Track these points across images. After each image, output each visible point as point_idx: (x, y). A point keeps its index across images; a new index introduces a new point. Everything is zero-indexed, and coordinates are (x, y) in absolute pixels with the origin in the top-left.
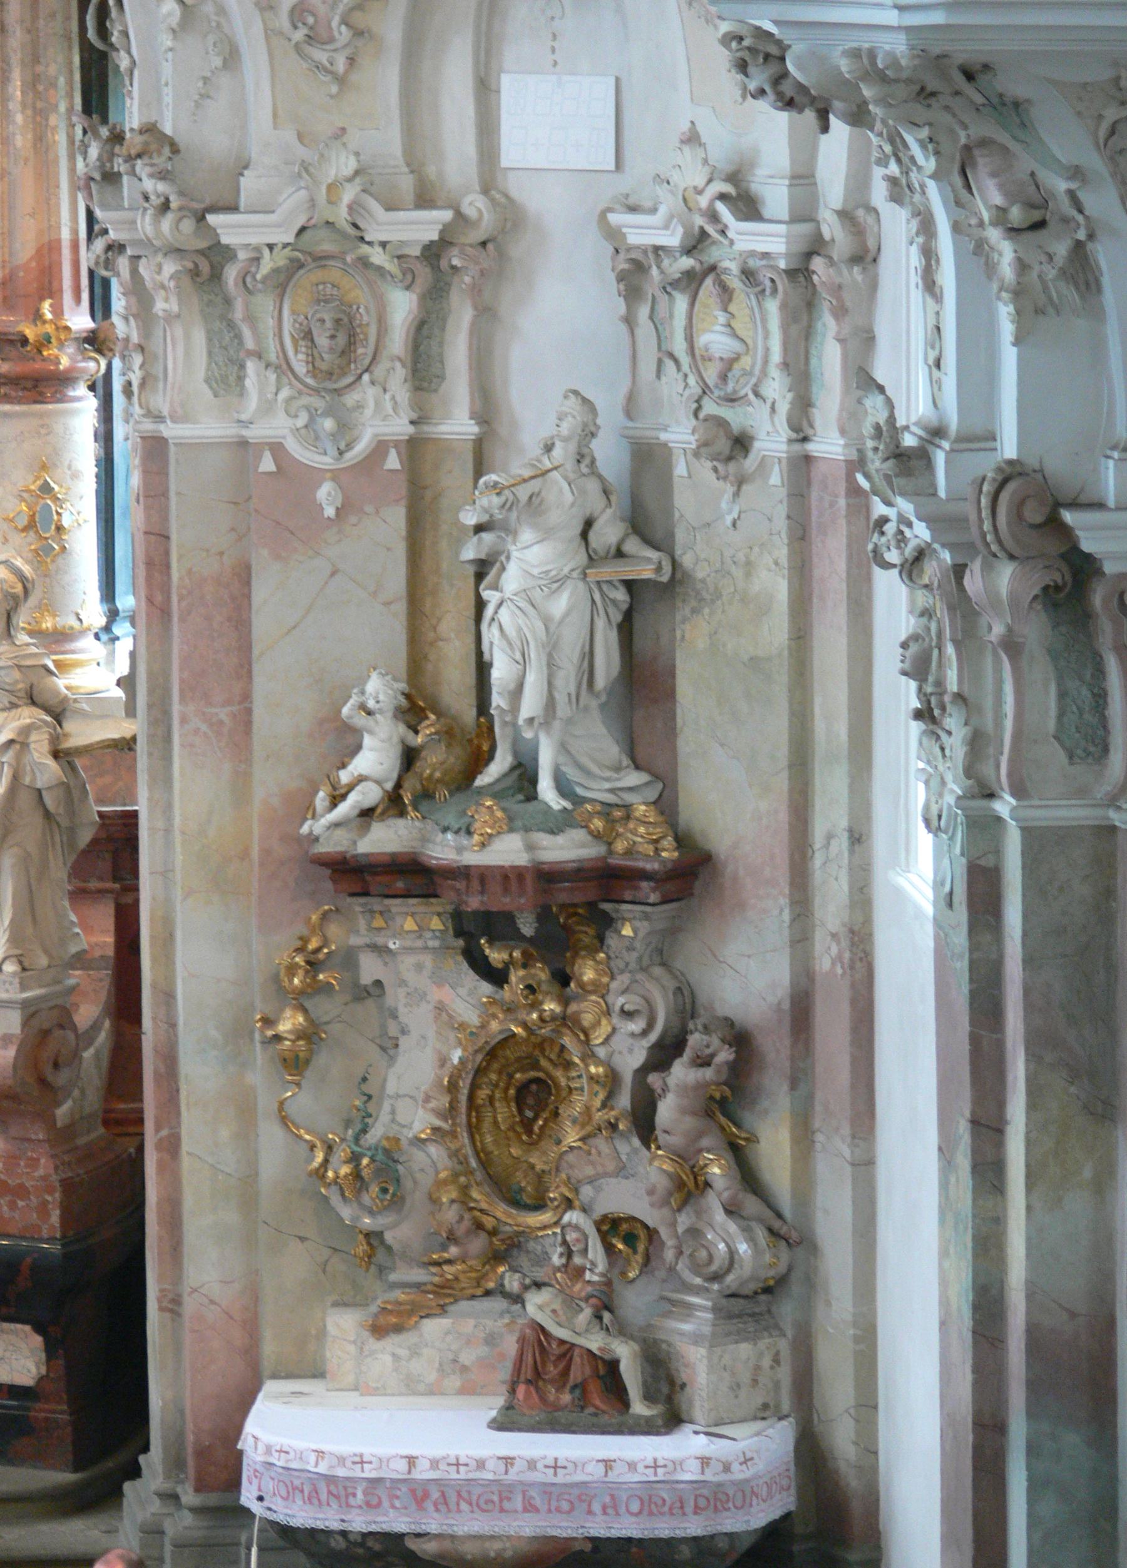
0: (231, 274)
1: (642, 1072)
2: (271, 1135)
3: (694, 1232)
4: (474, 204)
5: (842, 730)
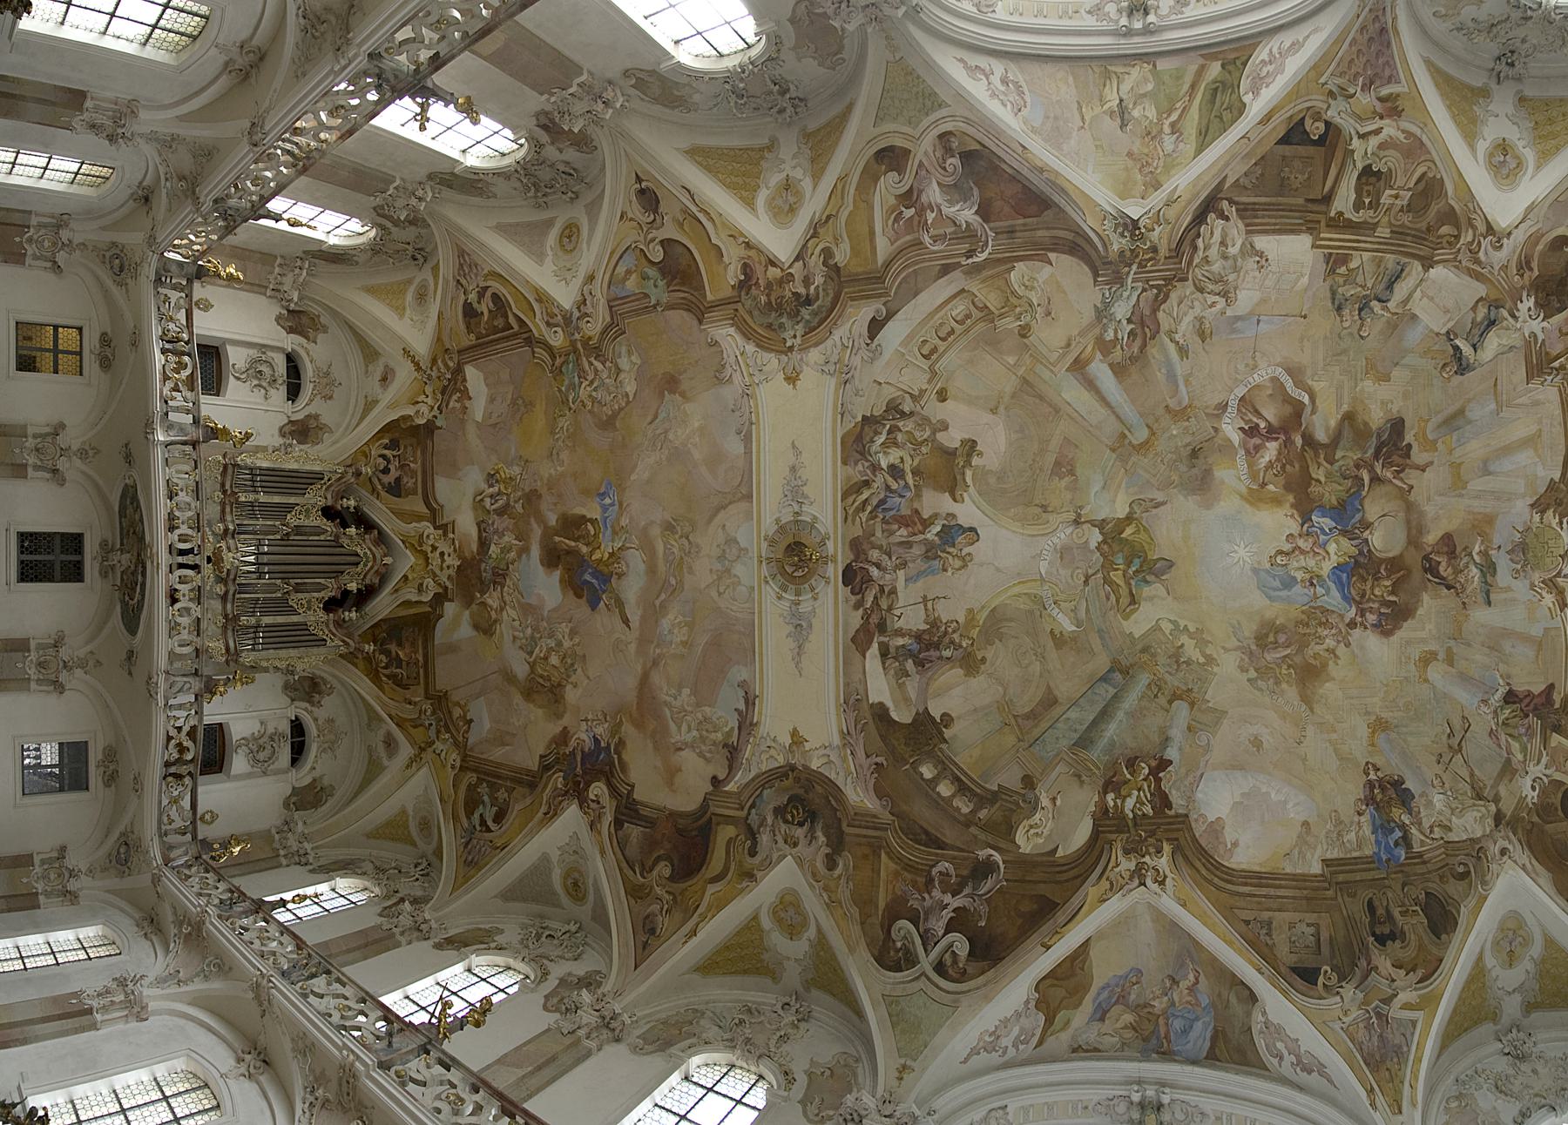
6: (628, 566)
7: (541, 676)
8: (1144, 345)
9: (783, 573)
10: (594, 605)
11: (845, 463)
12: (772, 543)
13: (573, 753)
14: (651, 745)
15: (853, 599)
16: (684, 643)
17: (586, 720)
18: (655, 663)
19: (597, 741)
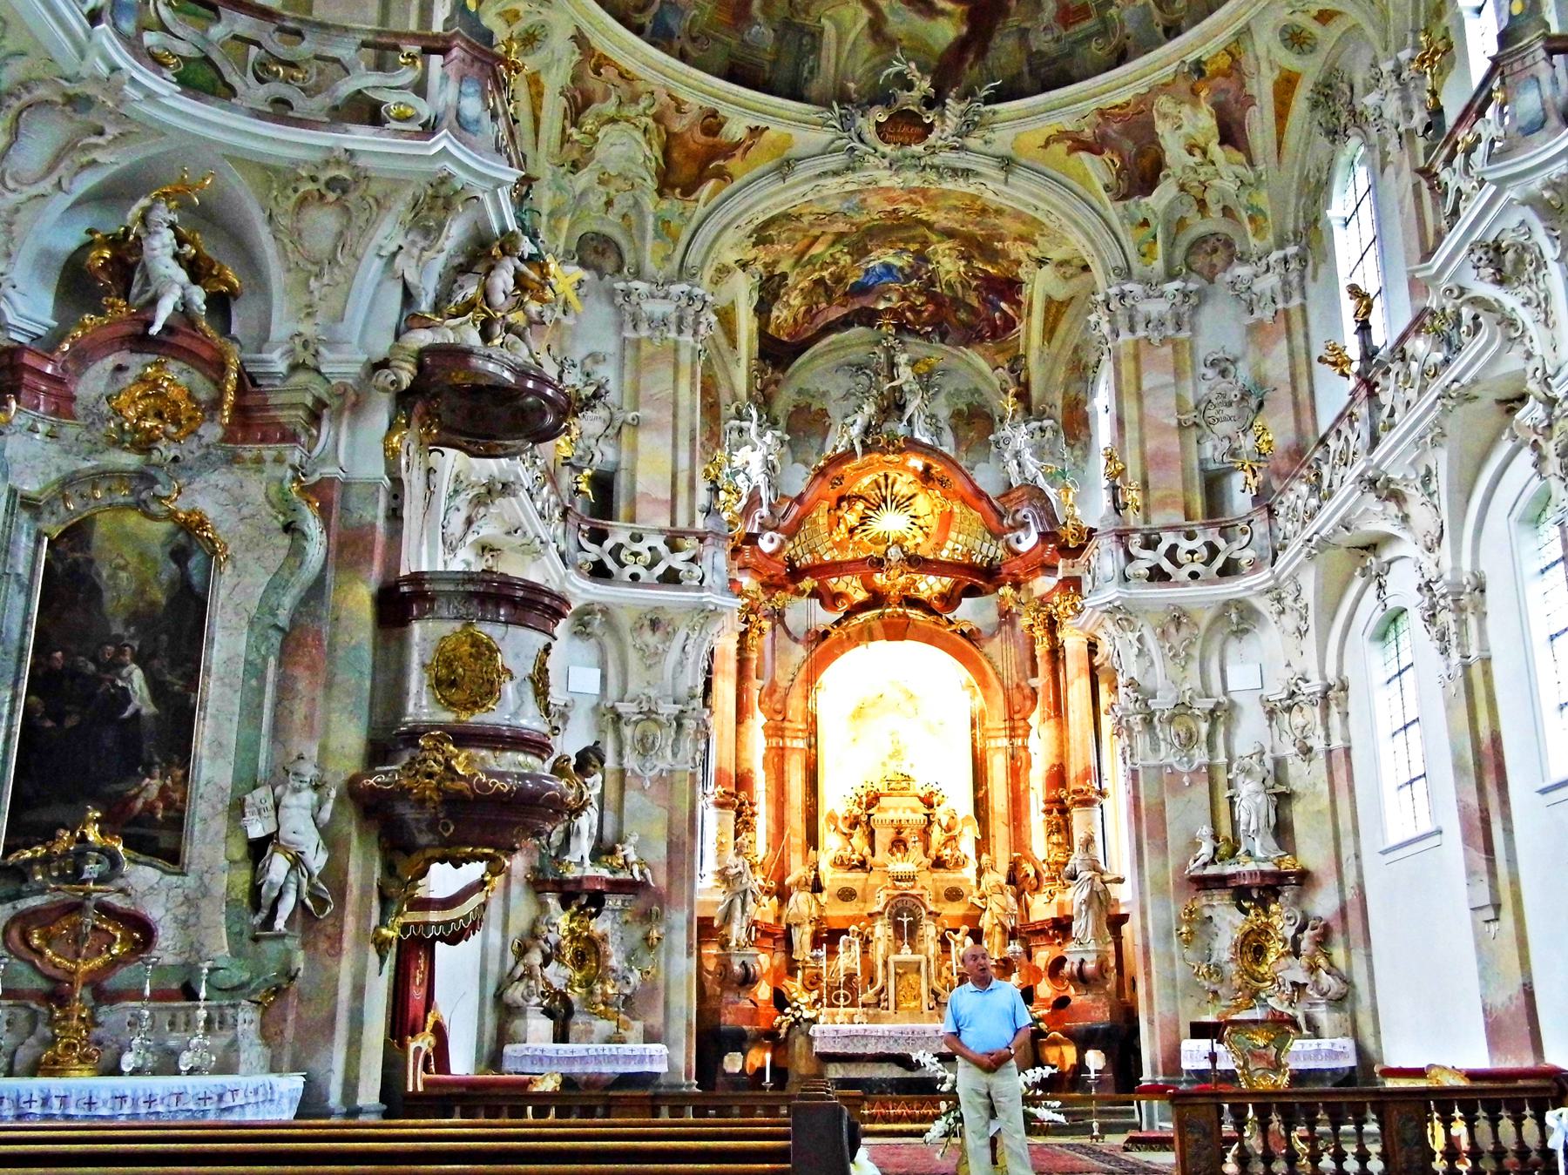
0: (1156, 720)
1: (1294, 937)
2: (1178, 963)
3: (1316, 982)
4: (1222, 699)
5: (1350, 827)
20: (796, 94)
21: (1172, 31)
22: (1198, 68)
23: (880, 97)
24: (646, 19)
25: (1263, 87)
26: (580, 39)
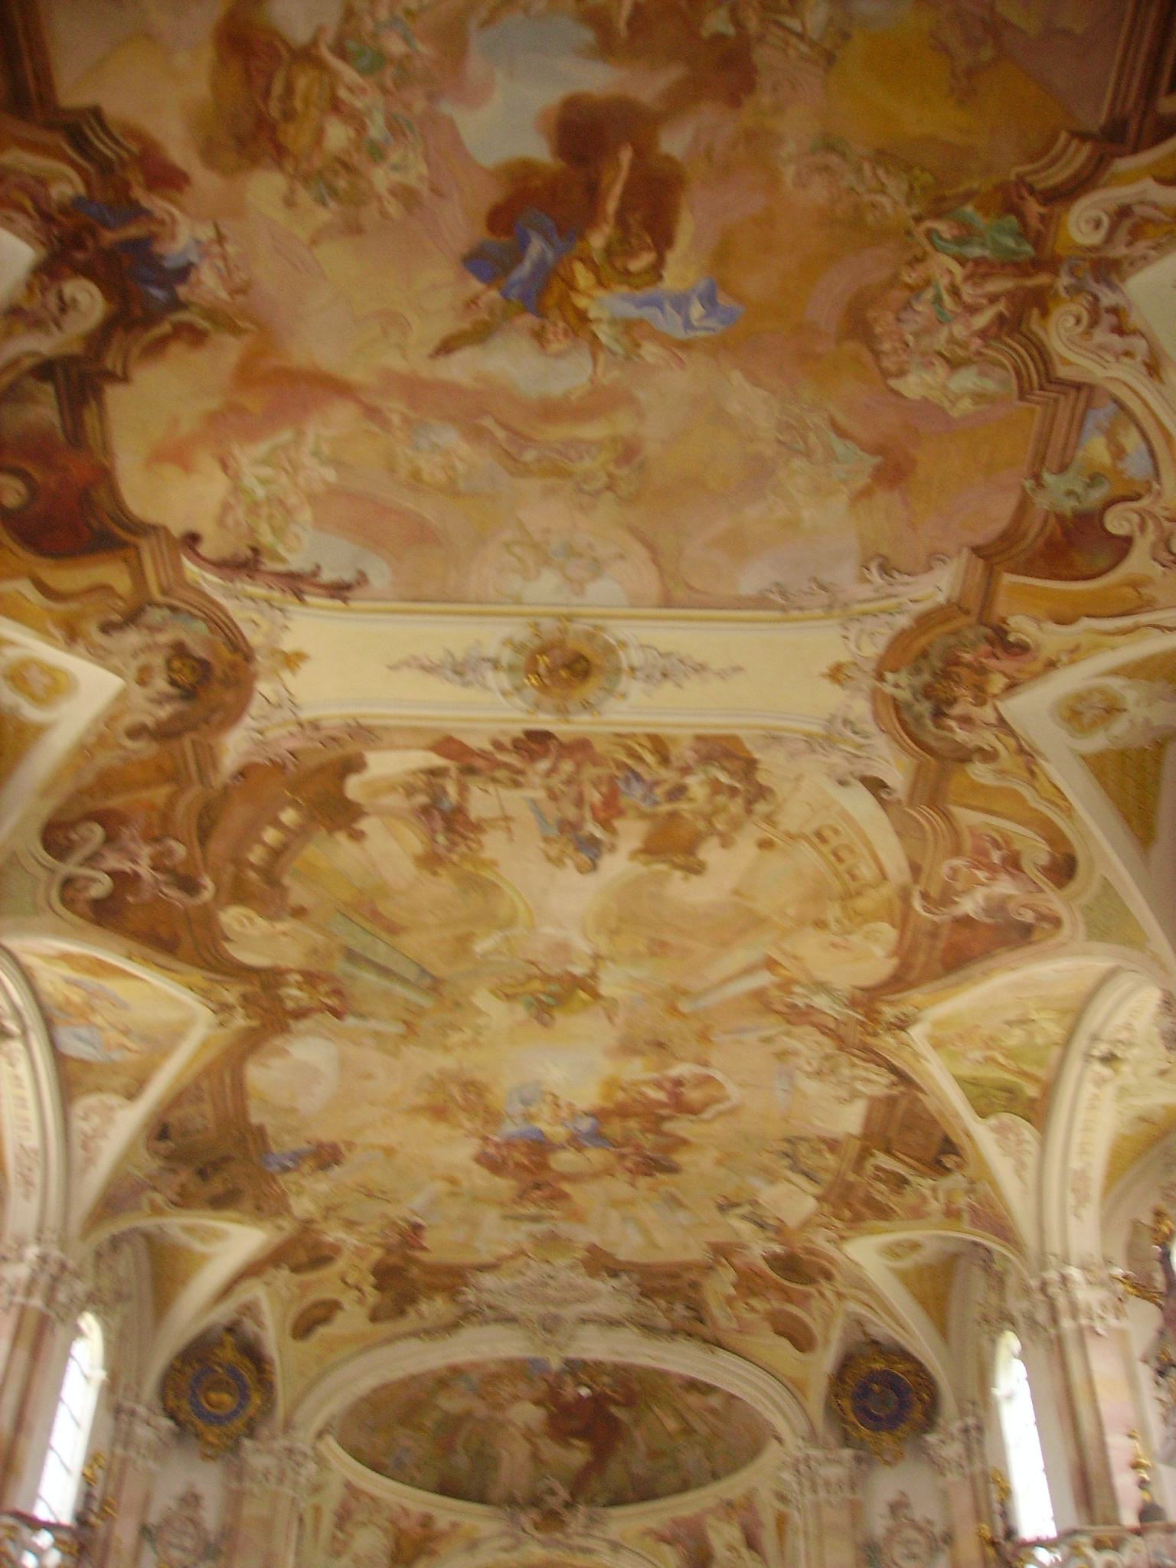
6: (558, 355)
7: (289, 90)
8: (777, 1012)
9: (543, 651)
10: (477, 262)
11: (700, 738)
12: (590, 637)
13: (138, 212)
14: (213, 403)
15: (507, 741)
16: (416, 475)
17: (221, 239)
18: (372, 413)
19: (184, 273)
20: (481, 1499)
21: (715, 1476)
22: (730, 1504)
23: (535, 1502)
24: (387, 1461)
25: (768, 1518)
26: (349, 1486)
